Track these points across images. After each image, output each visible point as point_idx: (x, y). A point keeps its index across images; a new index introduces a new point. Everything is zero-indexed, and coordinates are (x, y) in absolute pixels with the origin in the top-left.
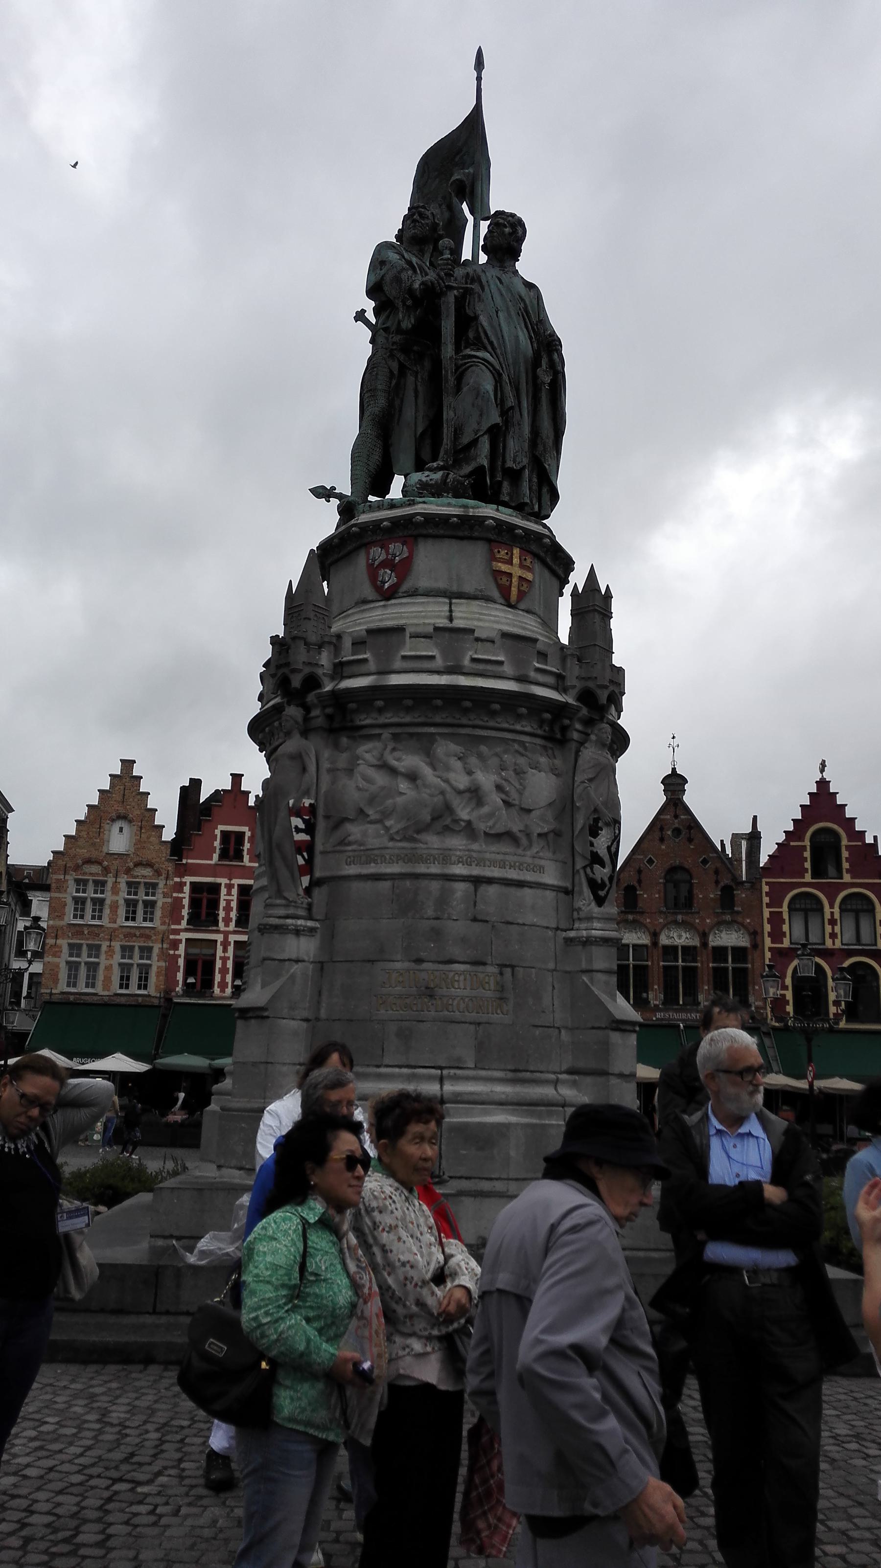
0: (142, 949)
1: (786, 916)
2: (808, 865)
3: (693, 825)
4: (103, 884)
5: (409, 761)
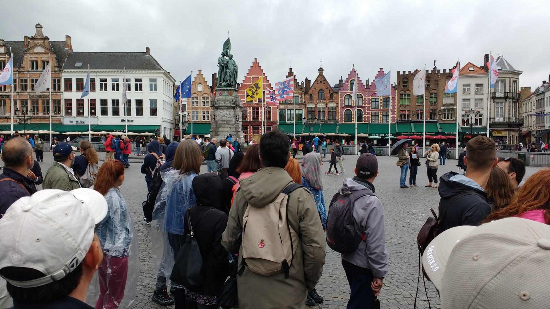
0: (207, 112)
1: (344, 100)
2: (349, 88)
3: (325, 80)
4: (197, 98)
5: (222, 111)
